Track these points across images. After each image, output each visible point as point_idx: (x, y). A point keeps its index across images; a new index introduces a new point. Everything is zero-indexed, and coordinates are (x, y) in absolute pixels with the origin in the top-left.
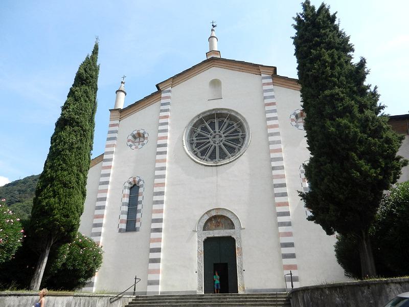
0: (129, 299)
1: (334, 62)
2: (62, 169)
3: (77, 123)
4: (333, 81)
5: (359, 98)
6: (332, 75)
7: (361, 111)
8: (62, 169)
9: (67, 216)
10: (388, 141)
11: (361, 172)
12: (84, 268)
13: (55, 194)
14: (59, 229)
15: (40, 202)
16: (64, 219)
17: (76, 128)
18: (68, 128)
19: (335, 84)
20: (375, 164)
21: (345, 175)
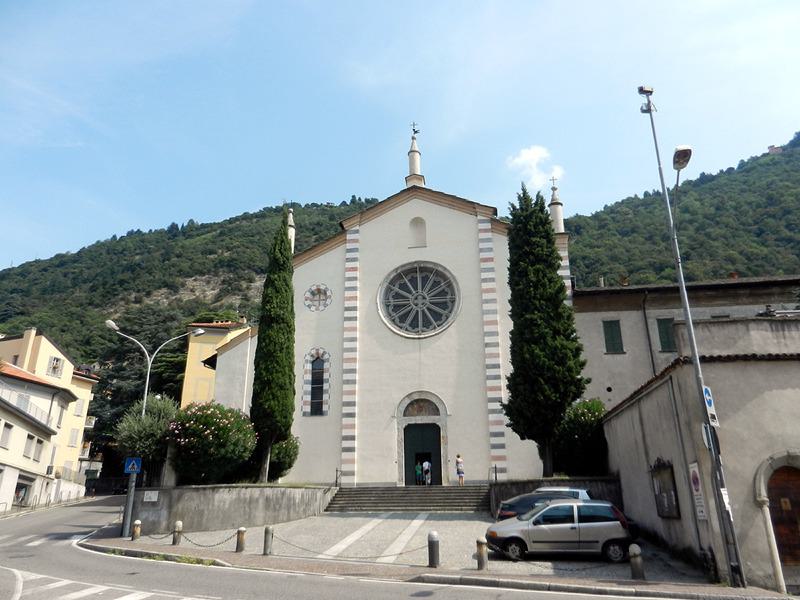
0: (335, 490)
1: (539, 281)
2: (277, 372)
3: (283, 319)
4: (535, 305)
5: (554, 324)
6: (534, 298)
7: (554, 338)
8: (277, 372)
9: (286, 417)
10: (570, 370)
11: (545, 396)
12: (288, 460)
13: (275, 397)
14: (280, 430)
15: (261, 404)
16: (284, 420)
17: (282, 325)
18: (274, 325)
19: (536, 308)
20: (557, 390)
21: (533, 396)
